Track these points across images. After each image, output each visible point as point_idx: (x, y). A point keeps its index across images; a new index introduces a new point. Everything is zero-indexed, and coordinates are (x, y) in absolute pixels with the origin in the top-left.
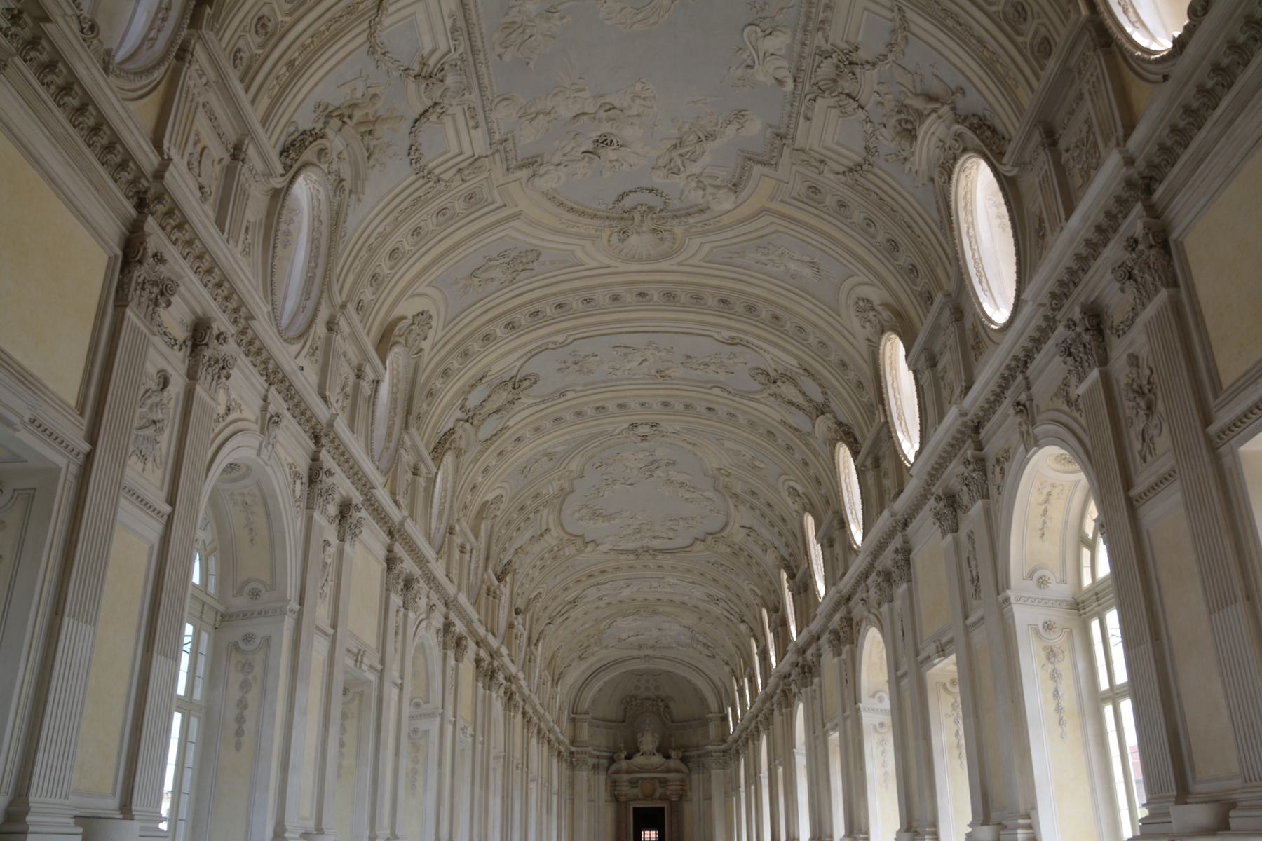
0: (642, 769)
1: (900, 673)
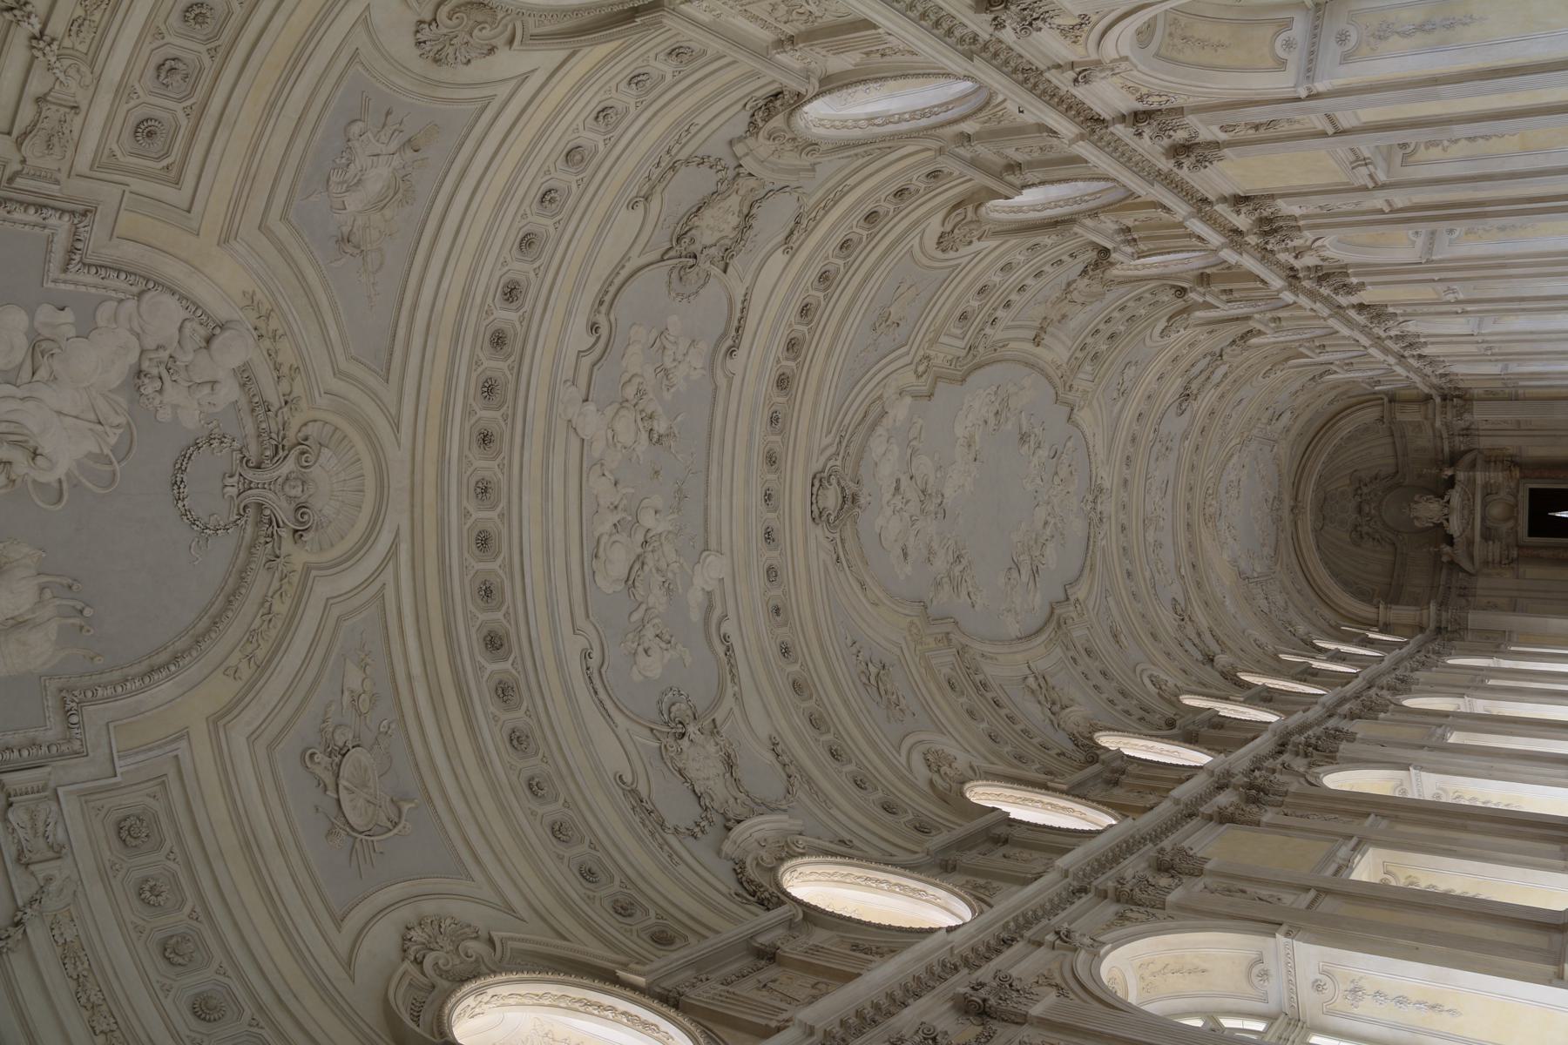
0: (1469, 523)
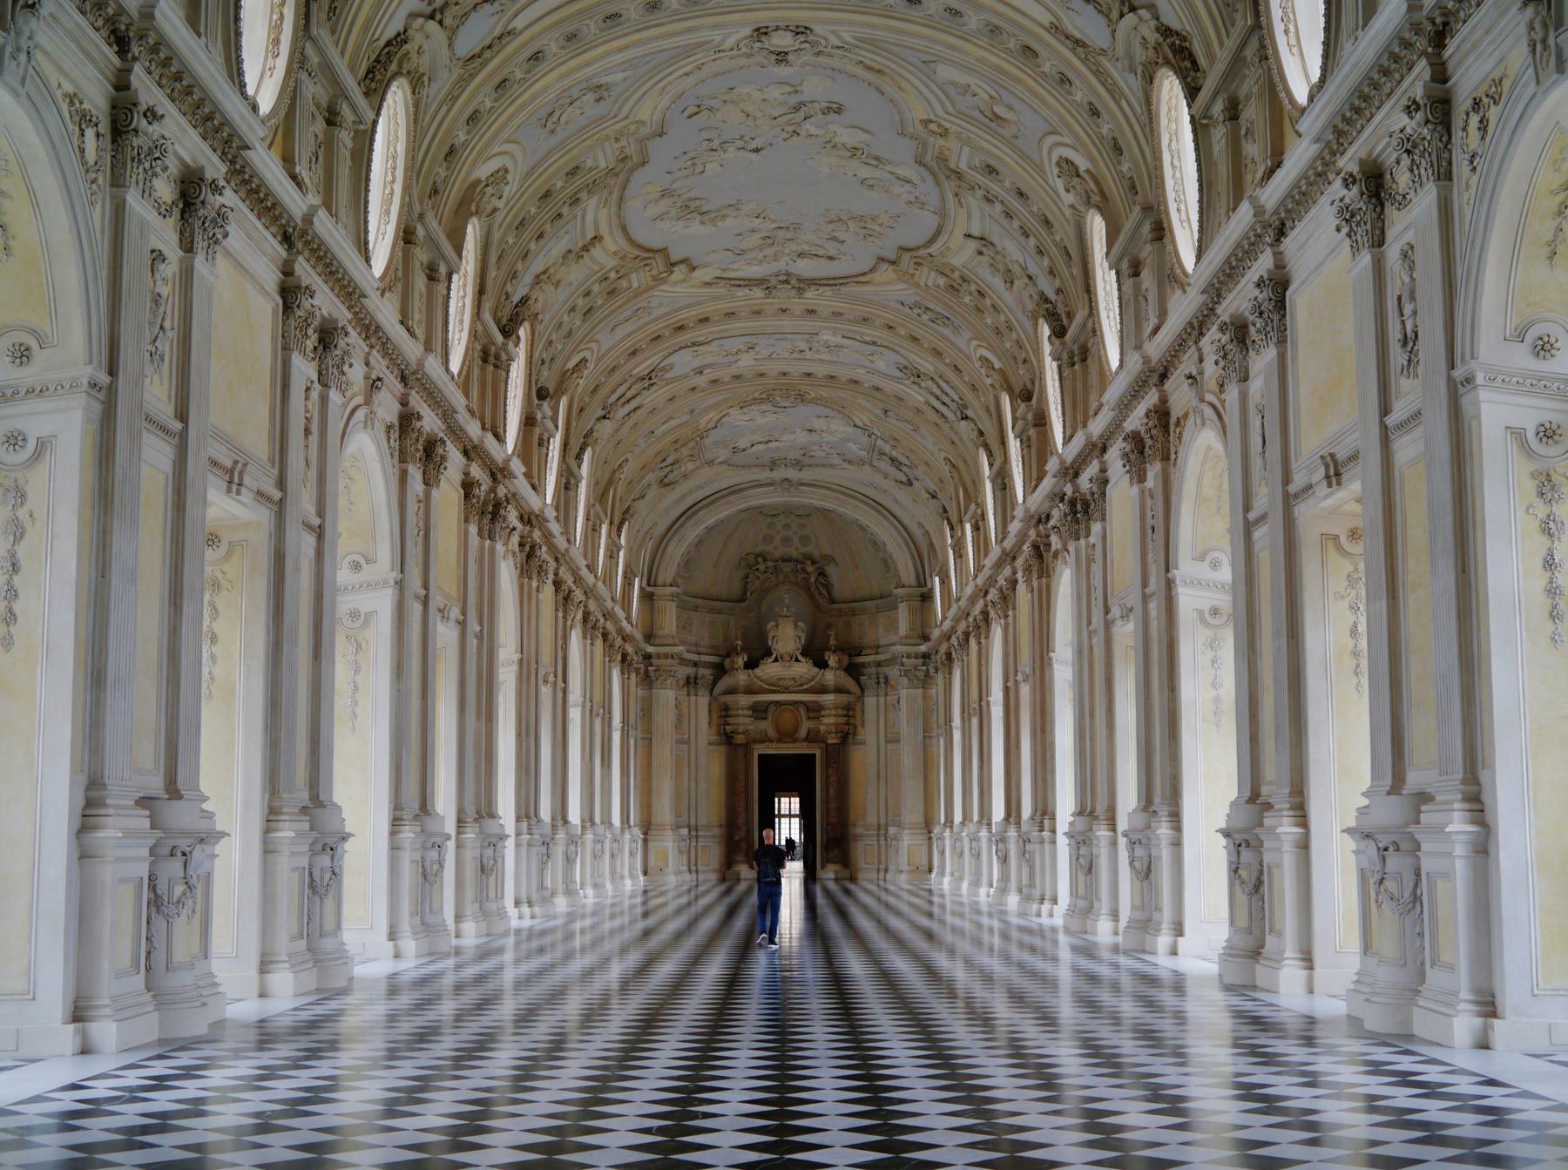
1: (1252, 516)
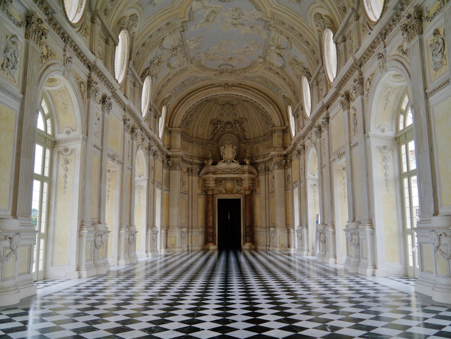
0: (223, 172)
